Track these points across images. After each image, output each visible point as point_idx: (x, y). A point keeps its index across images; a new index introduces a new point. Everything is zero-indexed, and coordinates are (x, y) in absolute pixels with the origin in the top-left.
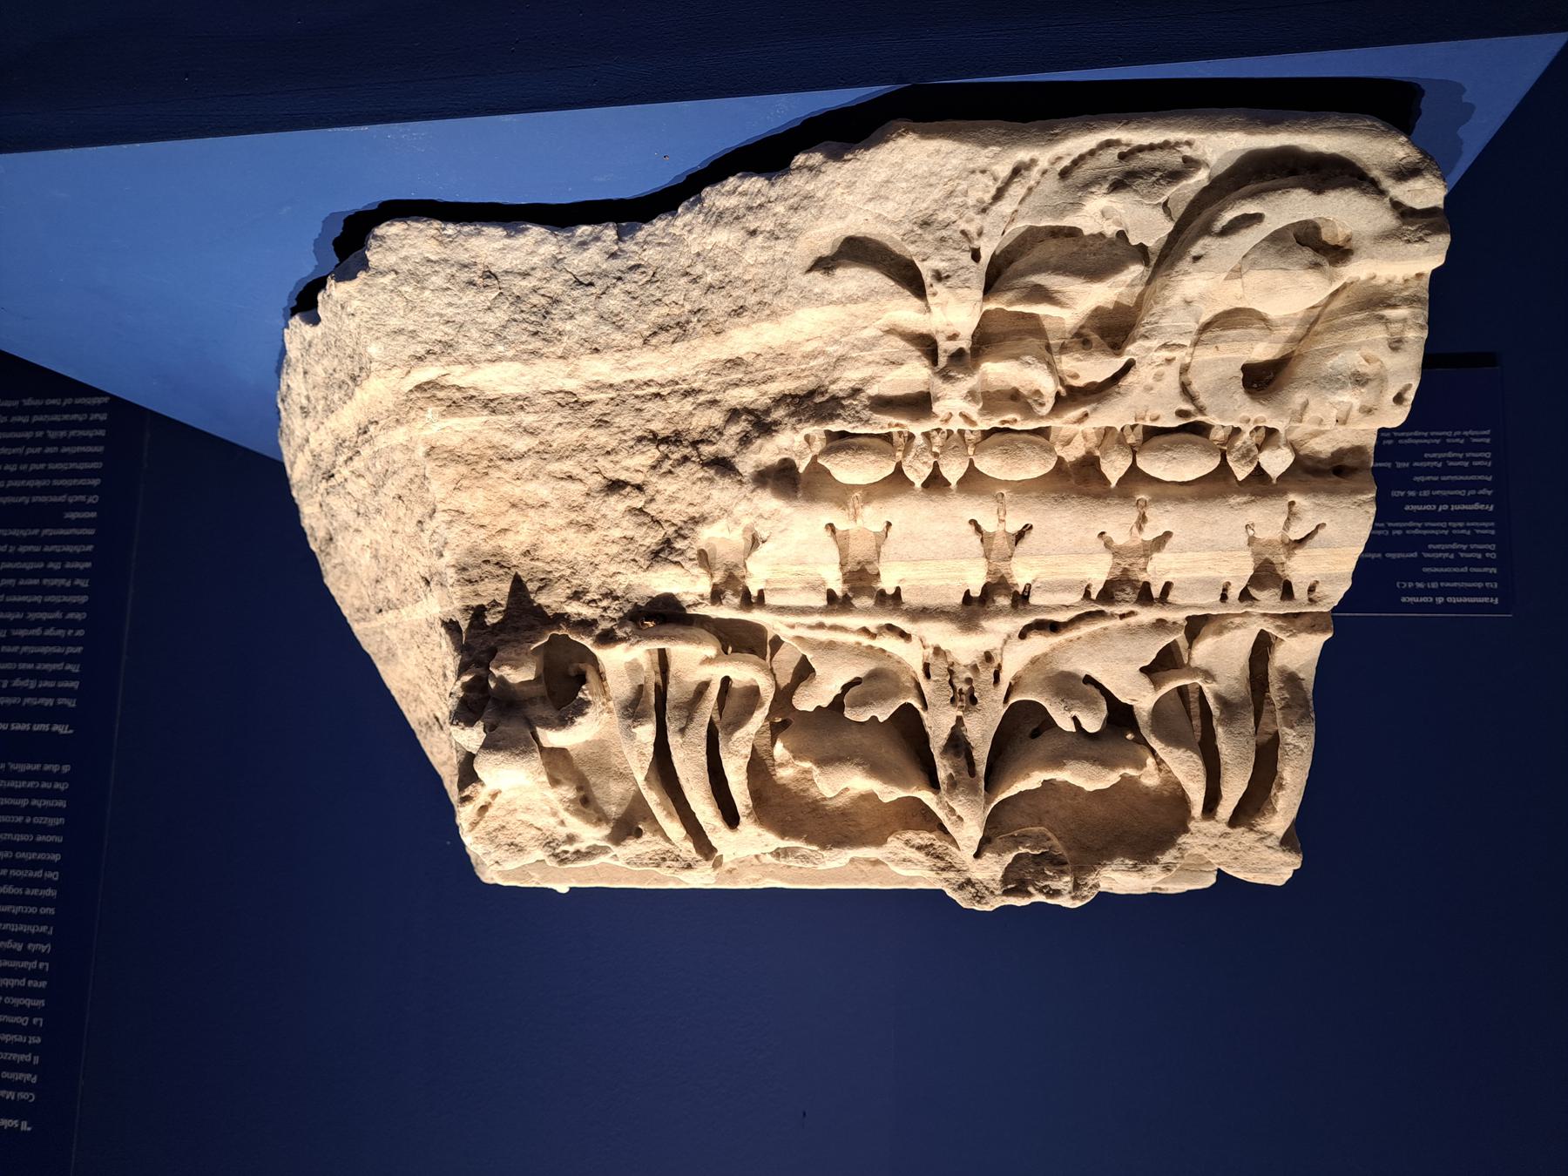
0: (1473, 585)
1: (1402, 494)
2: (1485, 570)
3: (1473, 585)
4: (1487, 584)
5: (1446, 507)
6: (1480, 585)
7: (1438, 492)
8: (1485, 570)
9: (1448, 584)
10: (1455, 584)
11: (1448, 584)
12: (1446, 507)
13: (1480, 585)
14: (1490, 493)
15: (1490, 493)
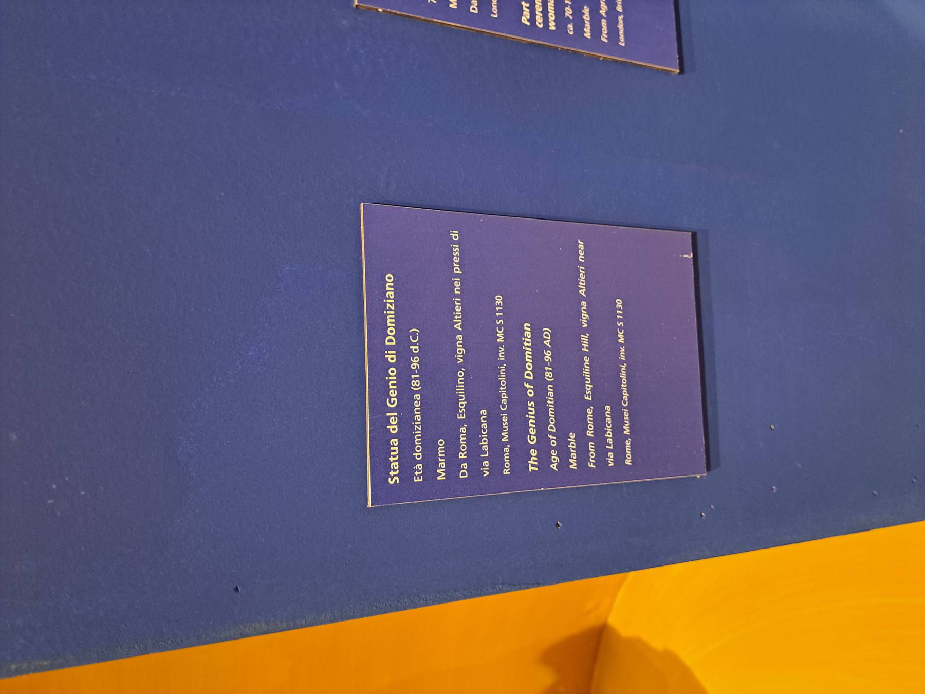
0: (418, 445)
1: (547, 343)
2: (442, 464)
3: (418, 445)
4: (419, 466)
5: (531, 393)
6: (418, 455)
7: (551, 394)
8: (442, 464)
9: (417, 405)
10: (418, 417)
11: (417, 405)
12: (531, 393)
13: (418, 455)
14: (553, 466)
15: (553, 466)
